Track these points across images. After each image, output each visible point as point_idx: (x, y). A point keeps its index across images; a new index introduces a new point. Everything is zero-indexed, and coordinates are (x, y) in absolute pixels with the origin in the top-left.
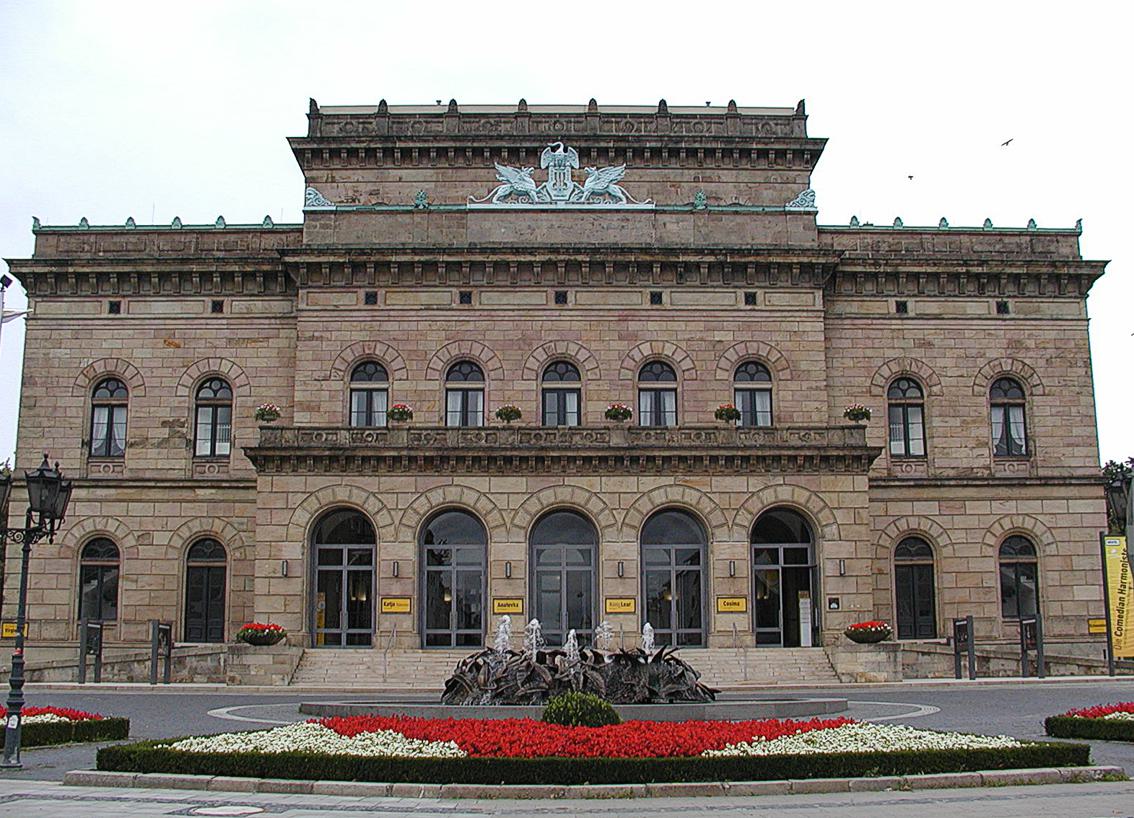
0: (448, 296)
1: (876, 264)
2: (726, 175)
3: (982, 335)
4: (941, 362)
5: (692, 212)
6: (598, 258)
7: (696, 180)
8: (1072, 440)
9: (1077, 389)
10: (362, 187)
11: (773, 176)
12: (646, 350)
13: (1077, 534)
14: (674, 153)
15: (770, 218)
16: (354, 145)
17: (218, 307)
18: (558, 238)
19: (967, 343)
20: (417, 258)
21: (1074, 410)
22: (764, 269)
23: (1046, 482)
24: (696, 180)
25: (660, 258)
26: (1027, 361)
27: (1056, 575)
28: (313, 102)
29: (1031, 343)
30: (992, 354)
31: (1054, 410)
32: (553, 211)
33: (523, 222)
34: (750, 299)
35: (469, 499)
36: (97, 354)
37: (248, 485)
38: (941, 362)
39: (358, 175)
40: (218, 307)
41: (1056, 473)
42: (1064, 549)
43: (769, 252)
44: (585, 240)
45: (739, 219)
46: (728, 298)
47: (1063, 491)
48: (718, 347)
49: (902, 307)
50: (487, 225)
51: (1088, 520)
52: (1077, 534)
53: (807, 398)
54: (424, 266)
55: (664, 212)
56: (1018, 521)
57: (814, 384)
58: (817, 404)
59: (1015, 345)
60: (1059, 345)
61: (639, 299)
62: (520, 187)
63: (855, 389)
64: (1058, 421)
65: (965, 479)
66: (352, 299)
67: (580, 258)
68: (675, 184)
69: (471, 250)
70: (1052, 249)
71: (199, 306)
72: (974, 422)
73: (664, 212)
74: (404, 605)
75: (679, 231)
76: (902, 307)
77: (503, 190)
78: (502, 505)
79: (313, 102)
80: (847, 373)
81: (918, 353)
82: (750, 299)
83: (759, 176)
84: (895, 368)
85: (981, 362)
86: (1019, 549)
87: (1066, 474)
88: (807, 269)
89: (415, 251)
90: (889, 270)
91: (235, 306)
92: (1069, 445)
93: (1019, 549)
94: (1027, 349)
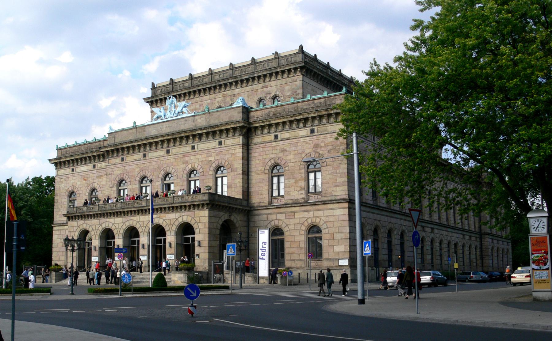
0: (139, 156)
1: (263, 122)
2: (273, 83)
3: (304, 144)
4: (289, 157)
5: (204, 114)
6: (174, 136)
7: (263, 87)
8: (337, 184)
9: (340, 162)
11: (289, 80)
12: (190, 167)
13: (337, 224)
15: (228, 111)
16: (161, 97)
18: (168, 131)
19: (299, 148)
20: (130, 145)
21: (338, 171)
23: (324, 203)
24: (263, 87)
25: (191, 133)
26: (321, 152)
27: (327, 241)
28: (153, 84)
29: (322, 145)
30: (308, 151)
31: (330, 172)
32: (167, 121)
35: (110, 226)
36: (70, 185)
37: (66, 224)
38: (289, 157)
41: (329, 199)
42: (332, 230)
43: (227, 124)
44: (175, 130)
45: (218, 113)
46: (212, 144)
47: (331, 206)
48: (210, 163)
49: (276, 137)
50: (150, 129)
51: (341, 218)
52: (337, 224)
53: (236, 178)
55: (196, 115)
56: (314, 220)
57: (238, 173)
58: (239, 180)
59: (317, 146)
60: (333, 143)
61: (188, 148)
62: (160, 114)
63: (259, 172)
64: (331, 176)
65: (295, 204)
66: (118, 160)
67: (169, 137)
68: (256, 91)
69: (147, 139)
70: (333, 102)
71: (90, 166)
72: (300, 180)
73: (196, 115)
75: (201, 122)
76: (276, 137)
78: (117, 227)
79: (153, 84)
80: (257, 166)
81: (281, 155)
83: (284, 81)
84: (273, 162)
85: (303, 155)
86: (314, 230)
87: (333, 199)
89: (129, 143)
90: (268, 123)
92: (335, 186)
93: (314, 230)
94: (321, 147)
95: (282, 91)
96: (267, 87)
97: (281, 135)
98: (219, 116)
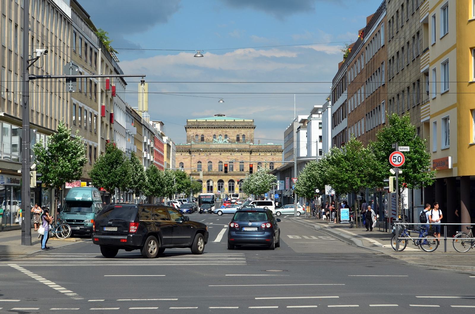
2: (243, 130)
10: (195, 132)
14: (236, 128)
17: (181, 154)
22: (243, 151)
33: (217, 145)
34: (242, 154)
39: (194, 130)
40: (181, 154)
49: (260, 154)
54: (205, 151)
68: (236, 132)
74: (205, 189)
76: (260, 154)
77: (214, 141)
81: (261, 160)
82: (242, 154)
83: (247, 130)
88: (248, 151)
91: (183, 154)
95: (246, 134)
96: (240, 131)
97: (261, 154)
98: (241, 146)
